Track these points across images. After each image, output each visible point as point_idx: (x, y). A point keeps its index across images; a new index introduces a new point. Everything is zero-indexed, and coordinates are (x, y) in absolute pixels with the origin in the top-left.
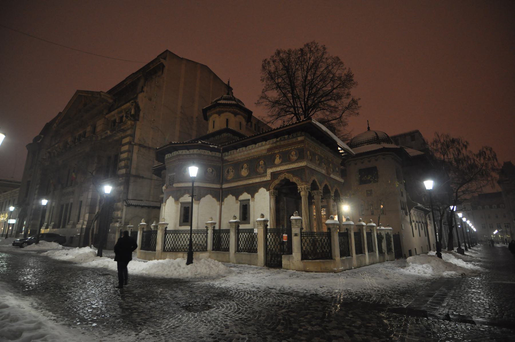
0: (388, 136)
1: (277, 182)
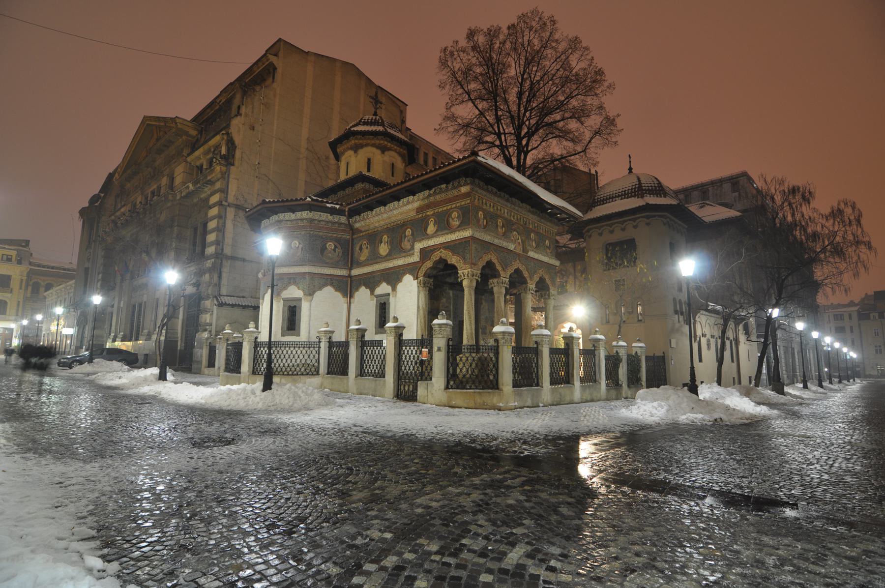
0: (659, 183)
1: (429, 264)
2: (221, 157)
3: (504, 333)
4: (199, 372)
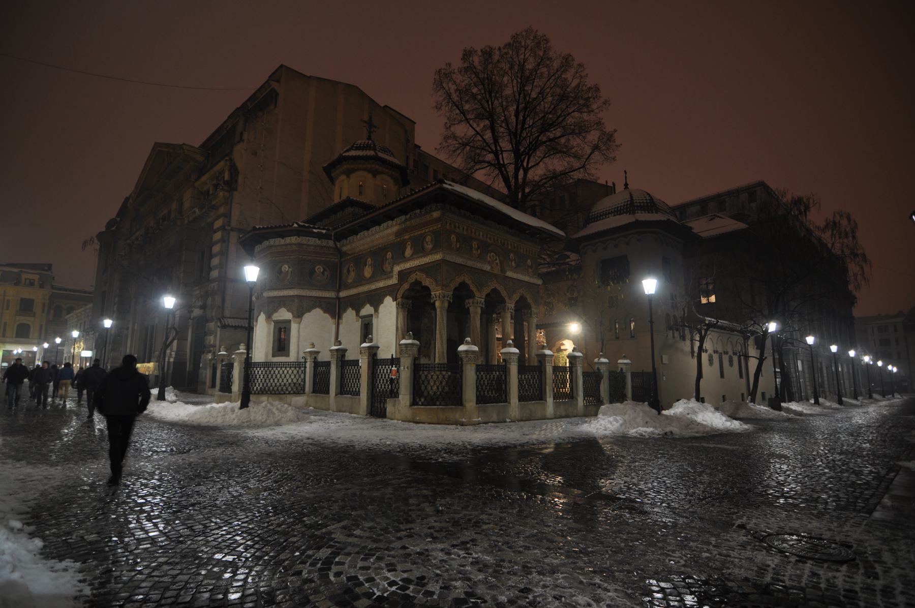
1: (406, 286)
2: (226, 183)
3: (466, 352)
4: (203, 393)
